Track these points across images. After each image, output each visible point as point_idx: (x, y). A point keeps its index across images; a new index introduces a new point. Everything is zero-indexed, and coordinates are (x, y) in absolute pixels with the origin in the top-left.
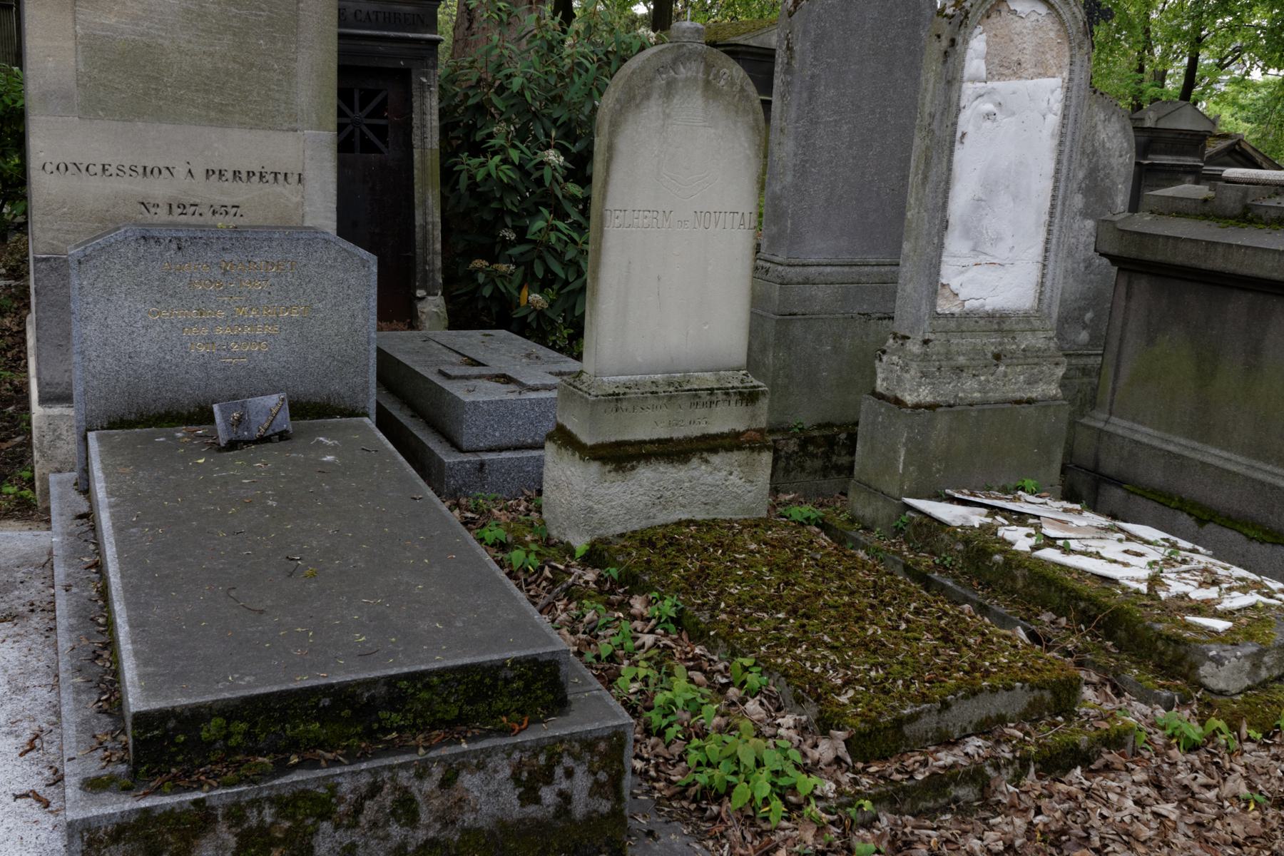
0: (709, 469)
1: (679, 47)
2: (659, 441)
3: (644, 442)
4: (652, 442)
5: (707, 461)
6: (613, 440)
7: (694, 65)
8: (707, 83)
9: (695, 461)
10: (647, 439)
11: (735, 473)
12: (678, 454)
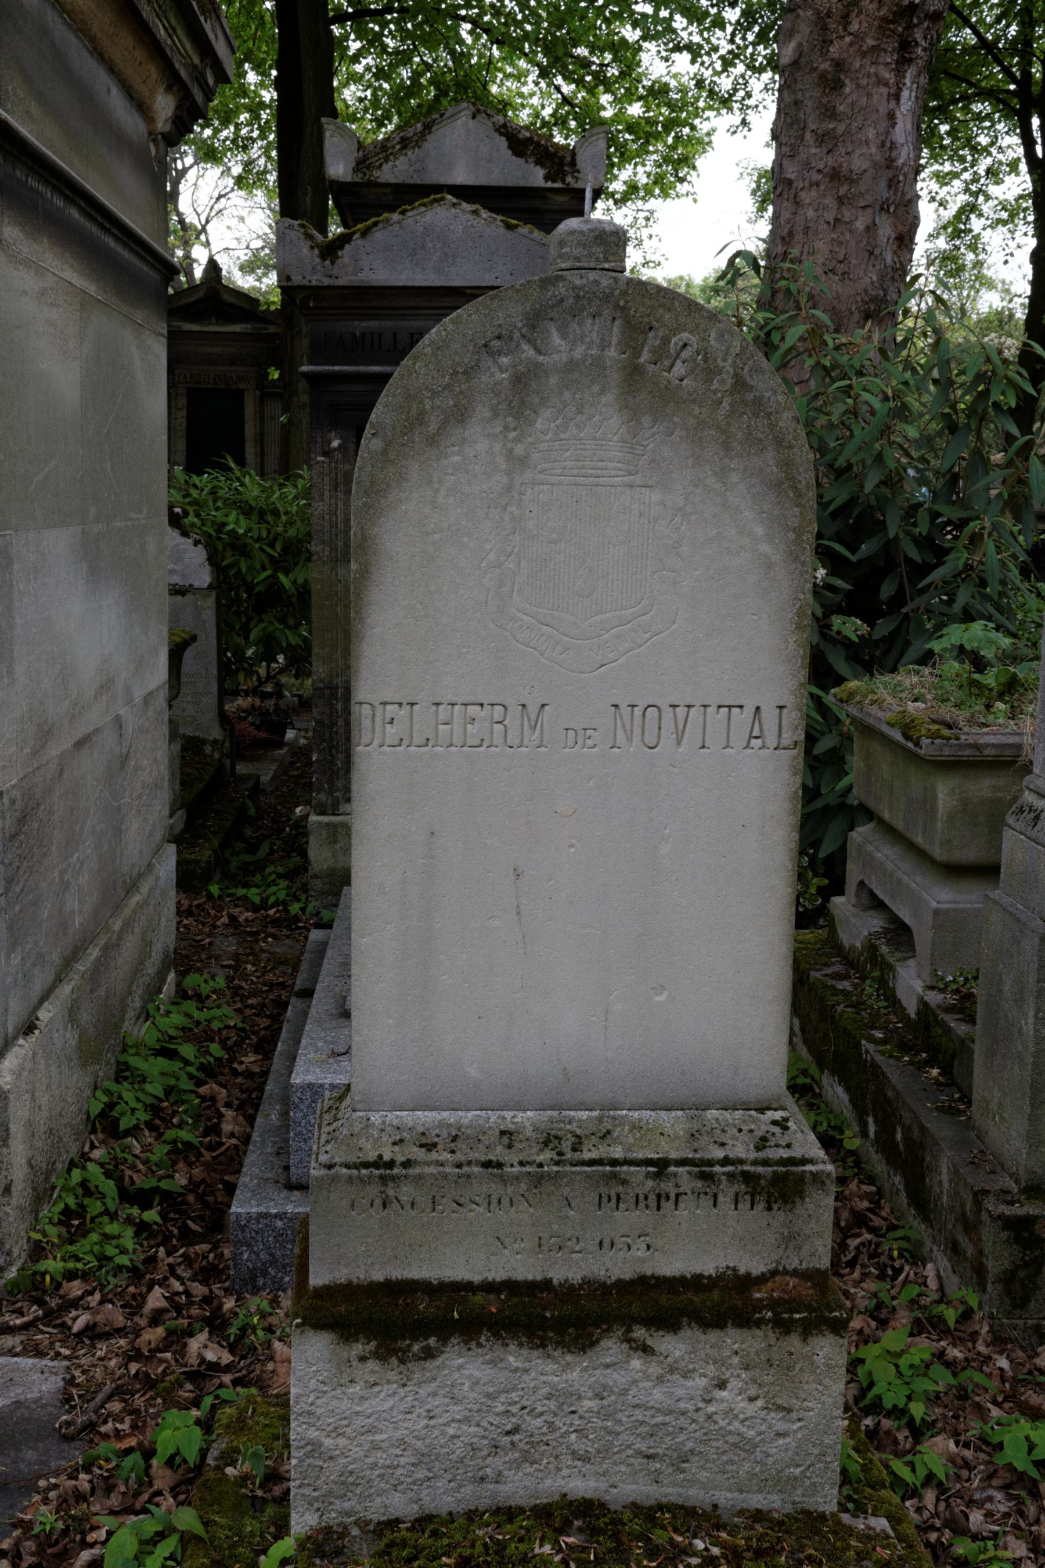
0: (655, 1370)
1: (546, 282)
2: (511, 1286)
3: (468, 1287)
4: (489, 1287)
5: (646, 1350)
6: (378, 1276)
7: (592, 329)
8: (633, 372)
9: (611, 1348)
10: (477, 1279)
11: (734, 1384)
12: (560, 1325)
